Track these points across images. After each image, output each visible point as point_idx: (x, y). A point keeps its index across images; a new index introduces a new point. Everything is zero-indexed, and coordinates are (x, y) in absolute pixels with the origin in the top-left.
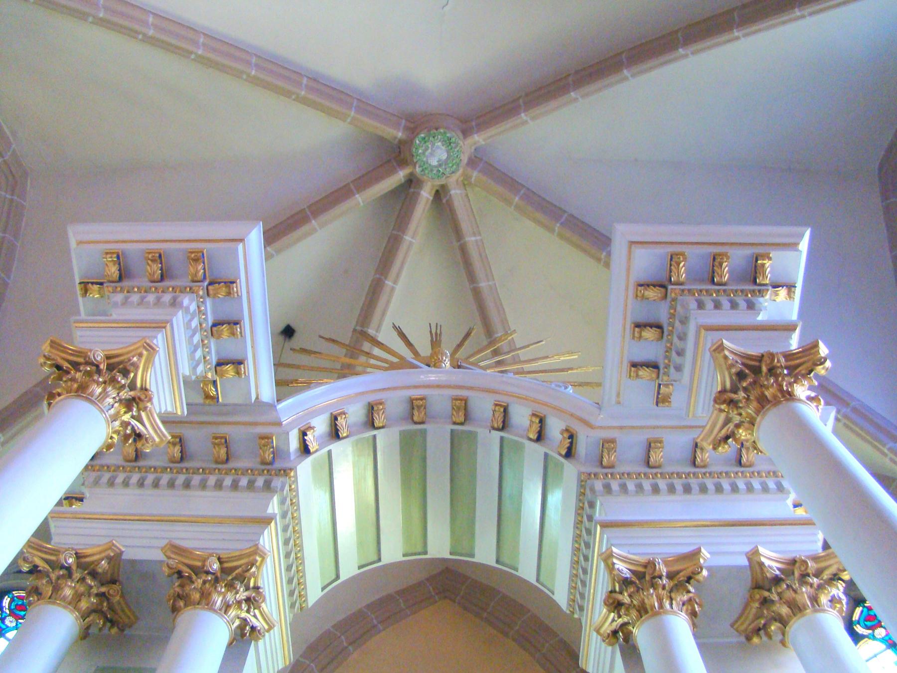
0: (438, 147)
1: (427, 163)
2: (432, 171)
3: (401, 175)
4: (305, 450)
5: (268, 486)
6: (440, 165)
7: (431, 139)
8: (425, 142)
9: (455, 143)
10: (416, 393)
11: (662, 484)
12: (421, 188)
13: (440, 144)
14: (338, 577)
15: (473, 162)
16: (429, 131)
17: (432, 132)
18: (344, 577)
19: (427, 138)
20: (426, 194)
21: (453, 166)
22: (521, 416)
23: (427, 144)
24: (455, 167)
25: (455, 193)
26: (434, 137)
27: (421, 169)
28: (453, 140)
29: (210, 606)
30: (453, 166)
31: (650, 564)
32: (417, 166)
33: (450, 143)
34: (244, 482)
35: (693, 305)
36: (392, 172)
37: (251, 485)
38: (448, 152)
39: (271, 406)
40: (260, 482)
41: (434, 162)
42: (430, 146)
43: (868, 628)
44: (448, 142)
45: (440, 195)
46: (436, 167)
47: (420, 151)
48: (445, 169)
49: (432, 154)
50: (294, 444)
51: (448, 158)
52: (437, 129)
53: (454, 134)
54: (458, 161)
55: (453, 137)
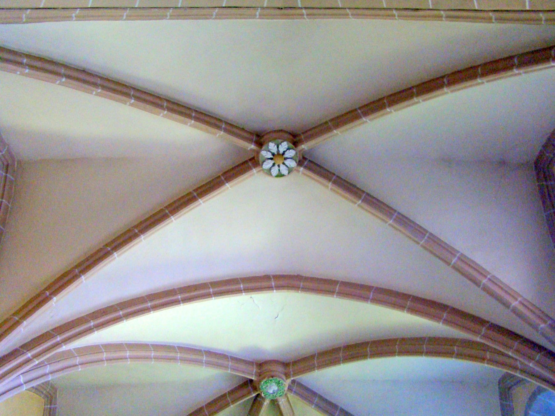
0: (273, 385)
1: (267, 392)
2: (270, 395)
3: (254, 395)
6: (274, 393)
7: (270, 381)
8: (267, 383)
9: (281, 383)
12: (264, 401)
13: (274, 384)
15: (290, 389)
16: (268, 378)
17: (270, 379)
19: (267, 382)
20: (266, 403)
21: (280, 393)
23: (268, 384)
24: (281, 393)
25: (282, 402)
26: (271, 381)
27: (264, 395)
28: (280, 382)
30: (280, 393)
32: (262, 393)
33: (279, 383)
36: (249, 393)
38: (278, 387)
41: (271, 391)
42: (269, 385)
44: (278, 383)
45: (274, 403)
46: (272, 393)
47: (264, 387)
48: (277, 394)
49: (270, 387)
51: (278, 390)
52: (272, 377)
53: (280, 379)
54: (283, 391)
55: (281, 381)
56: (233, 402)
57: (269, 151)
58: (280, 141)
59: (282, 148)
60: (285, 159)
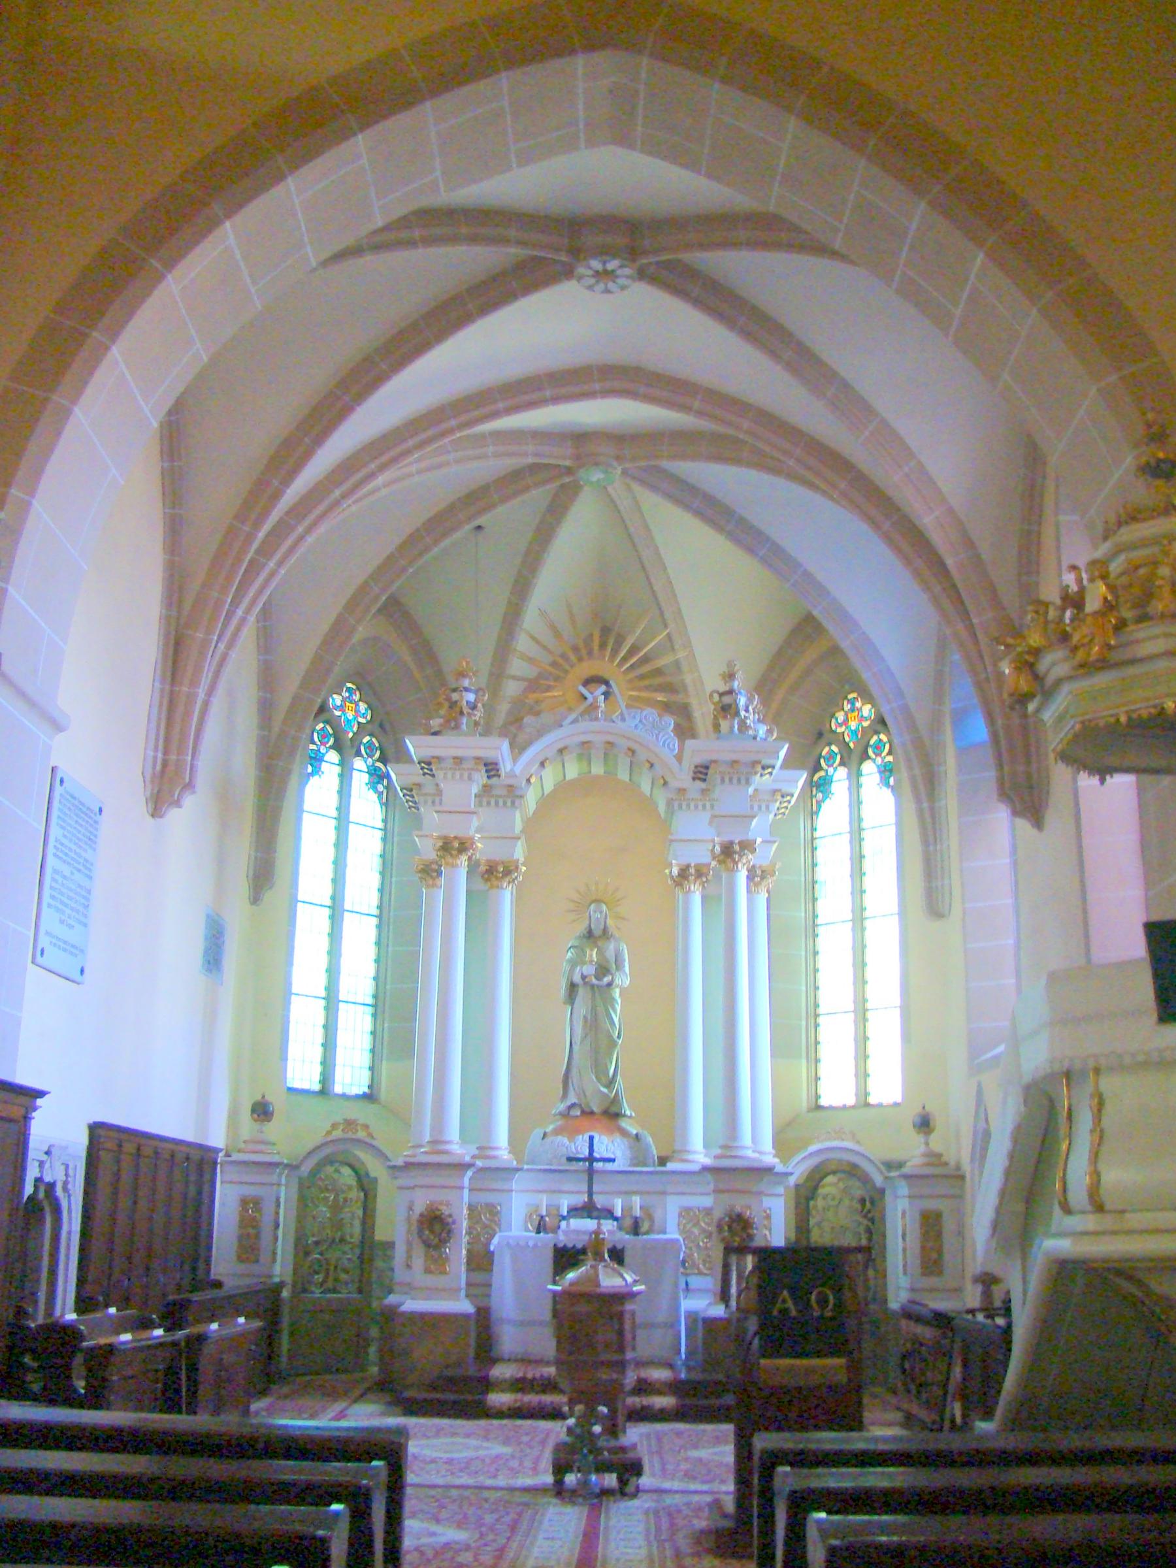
4: (528, 781)
5: (513, 803)
10: (584, 738)
11: (708, 804)
14: (543, 794)
18: (546, 793)
22: (642, 755)
29: (502, 888)
31: (688, 866)
34: (501, 803)
35: (719, 781)
37: (505, 803)
39: (512, 770)
40: (509, 804)
43: (874, 753)
50: (524, 782)
56: (537, 485)
57: (590, 268)
58: (608, 258)
59: (611, 266)
60: (617, 277)
